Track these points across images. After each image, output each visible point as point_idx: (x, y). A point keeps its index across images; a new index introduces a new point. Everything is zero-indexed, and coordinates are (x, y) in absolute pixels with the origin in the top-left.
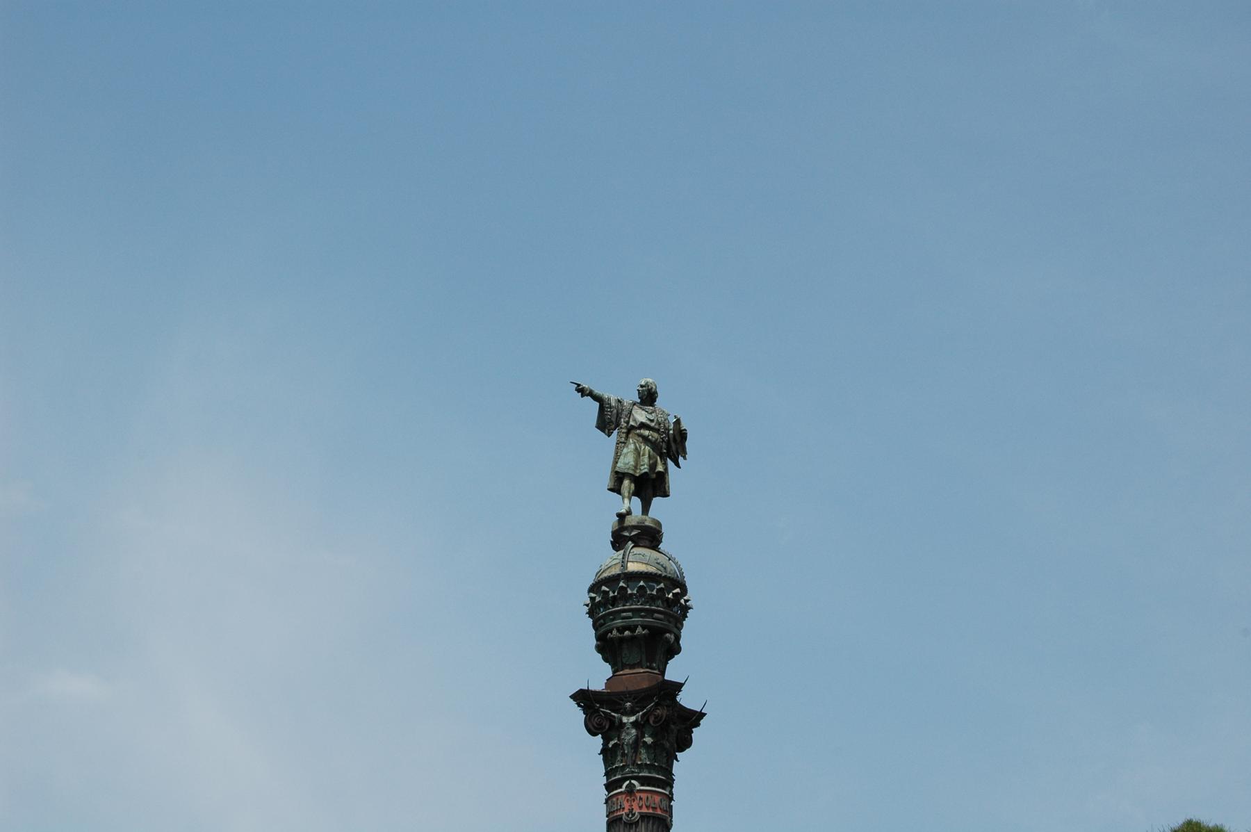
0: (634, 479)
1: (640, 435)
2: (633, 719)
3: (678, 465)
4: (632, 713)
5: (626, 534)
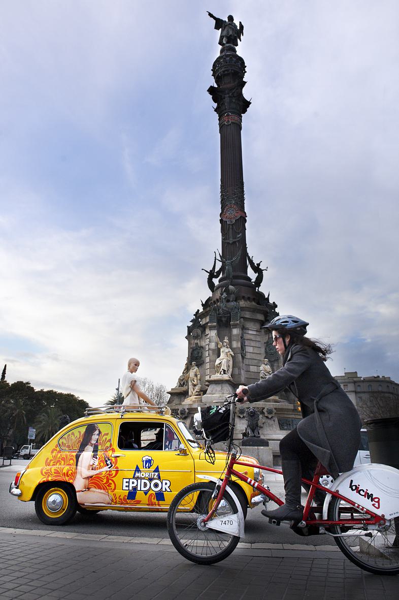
3: (241, 41)
4: (228, 94)
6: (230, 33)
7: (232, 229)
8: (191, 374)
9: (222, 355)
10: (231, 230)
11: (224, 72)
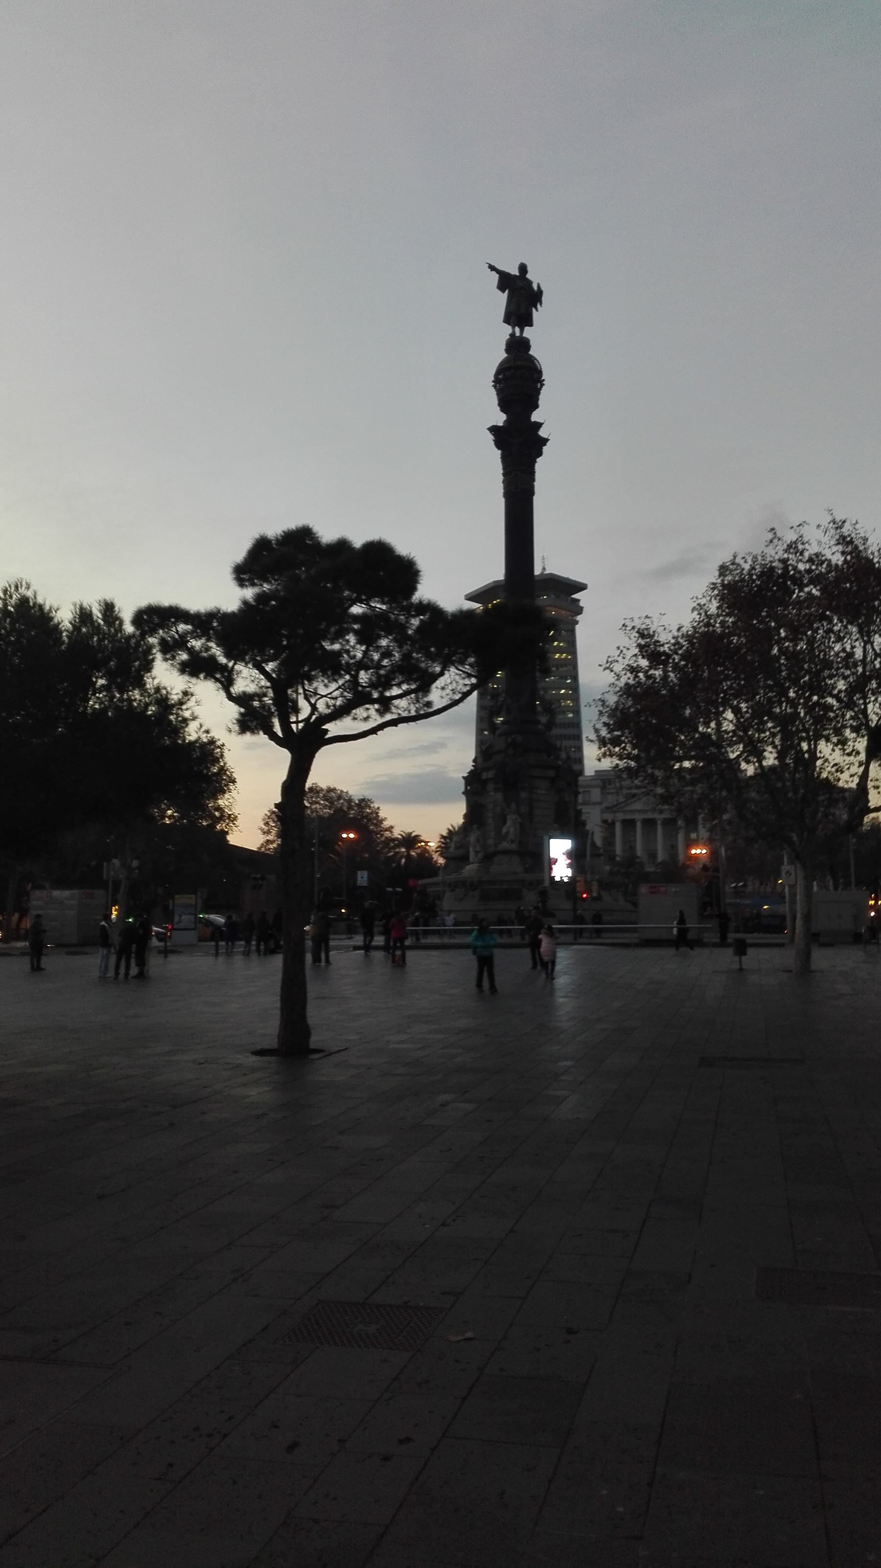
6: (521, 297)
8: (472, 838)
9: (509, 823)
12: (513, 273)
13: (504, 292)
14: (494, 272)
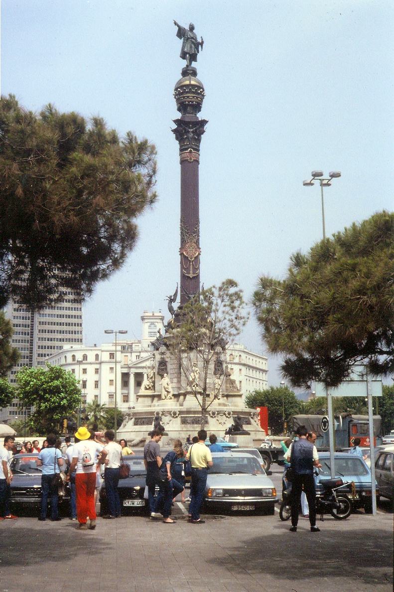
0: (190, 55)
1: (192, 41)
2: (192, 130)
5: (189, 72)
6: (191, 45)
7: (193, 265)
10: (191, 266)
11: (189, 102)
12: (186, 28)
13: (181, 39)
14: (176, 26)
